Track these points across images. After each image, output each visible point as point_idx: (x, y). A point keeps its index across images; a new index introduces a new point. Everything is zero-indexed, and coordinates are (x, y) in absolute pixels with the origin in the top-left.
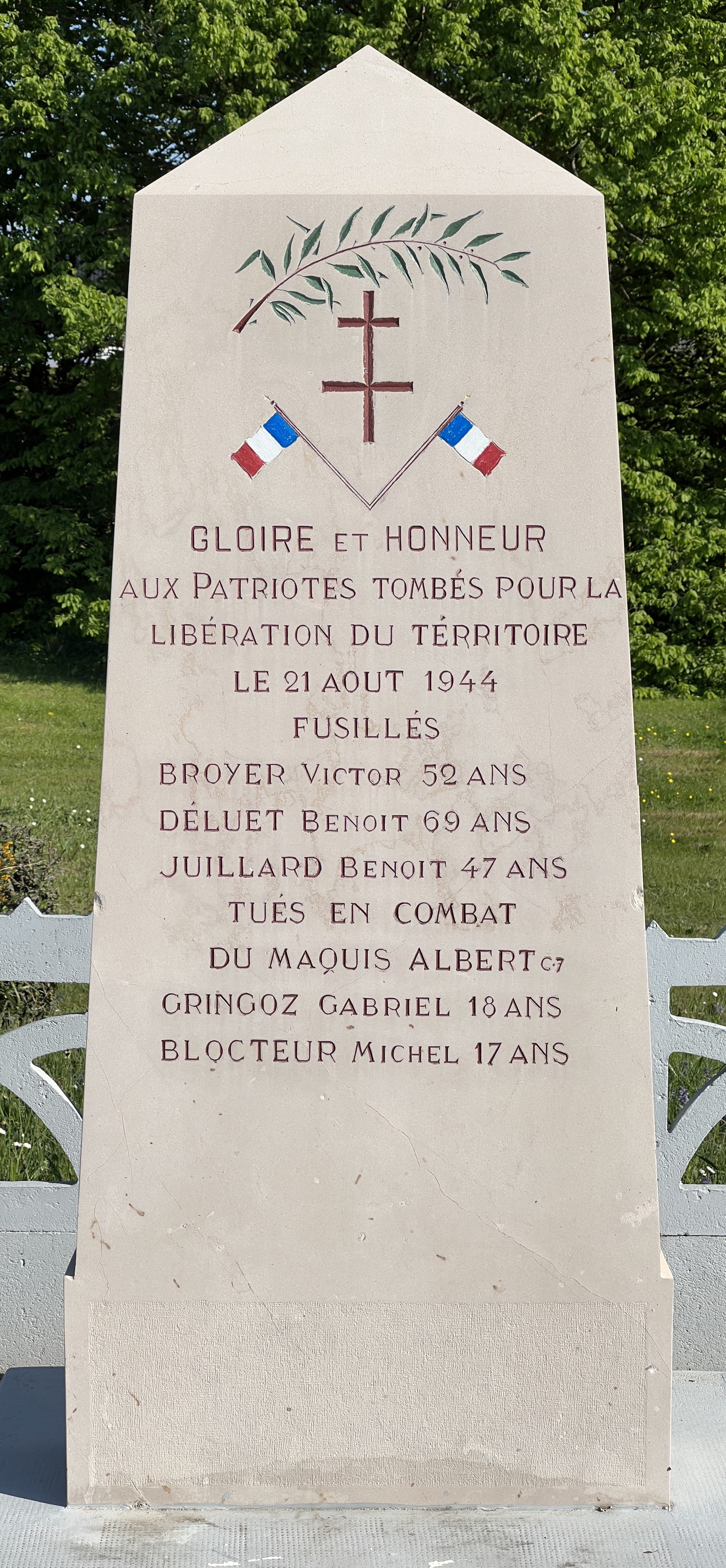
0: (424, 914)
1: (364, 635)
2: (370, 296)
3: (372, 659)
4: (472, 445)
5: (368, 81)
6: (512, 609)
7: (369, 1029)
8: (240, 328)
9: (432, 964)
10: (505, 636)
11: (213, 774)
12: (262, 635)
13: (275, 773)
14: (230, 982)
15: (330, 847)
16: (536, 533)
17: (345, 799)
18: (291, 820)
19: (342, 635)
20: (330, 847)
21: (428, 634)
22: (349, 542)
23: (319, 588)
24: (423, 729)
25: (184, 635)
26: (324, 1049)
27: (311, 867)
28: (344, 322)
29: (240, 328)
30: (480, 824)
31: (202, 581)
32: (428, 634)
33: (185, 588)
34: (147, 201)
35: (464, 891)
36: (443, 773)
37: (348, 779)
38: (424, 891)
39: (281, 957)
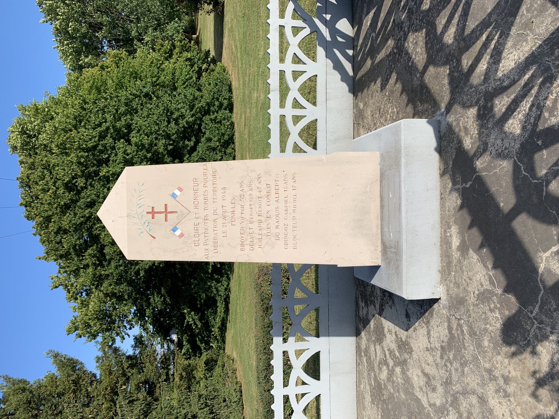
0: (268, 200)
1: (215, 213)
2: (147, 213)
3: (220, 211)
4: (177, 192)
6: (209, 184)
7: (290, 210)
8: (154, 238)
9: (278, 199)
10: (215, 186)
11: (243, 241)
12: (215, 232)
14: (282, 236)
15: (256, 218)
16: (195, 180)
17: (247, 216)
18: (251, 226)
19: (215, 217)
20: (256, 218)
21: (215, 200)
22: (197, 216)
23: (206, 221)
24: (233, 201)
25: (215, 247)
27: (260, 222)
28: (153, 218)
29: (154, 238)
30: (251, 190)
31: (205, 244)
32: (215, 200)
33: (206, 247)
34: (129, 256)
35: (264, 193)
36: (242, 197)
37: (243, 215)
38: (264, 201)
39: (277, 227)
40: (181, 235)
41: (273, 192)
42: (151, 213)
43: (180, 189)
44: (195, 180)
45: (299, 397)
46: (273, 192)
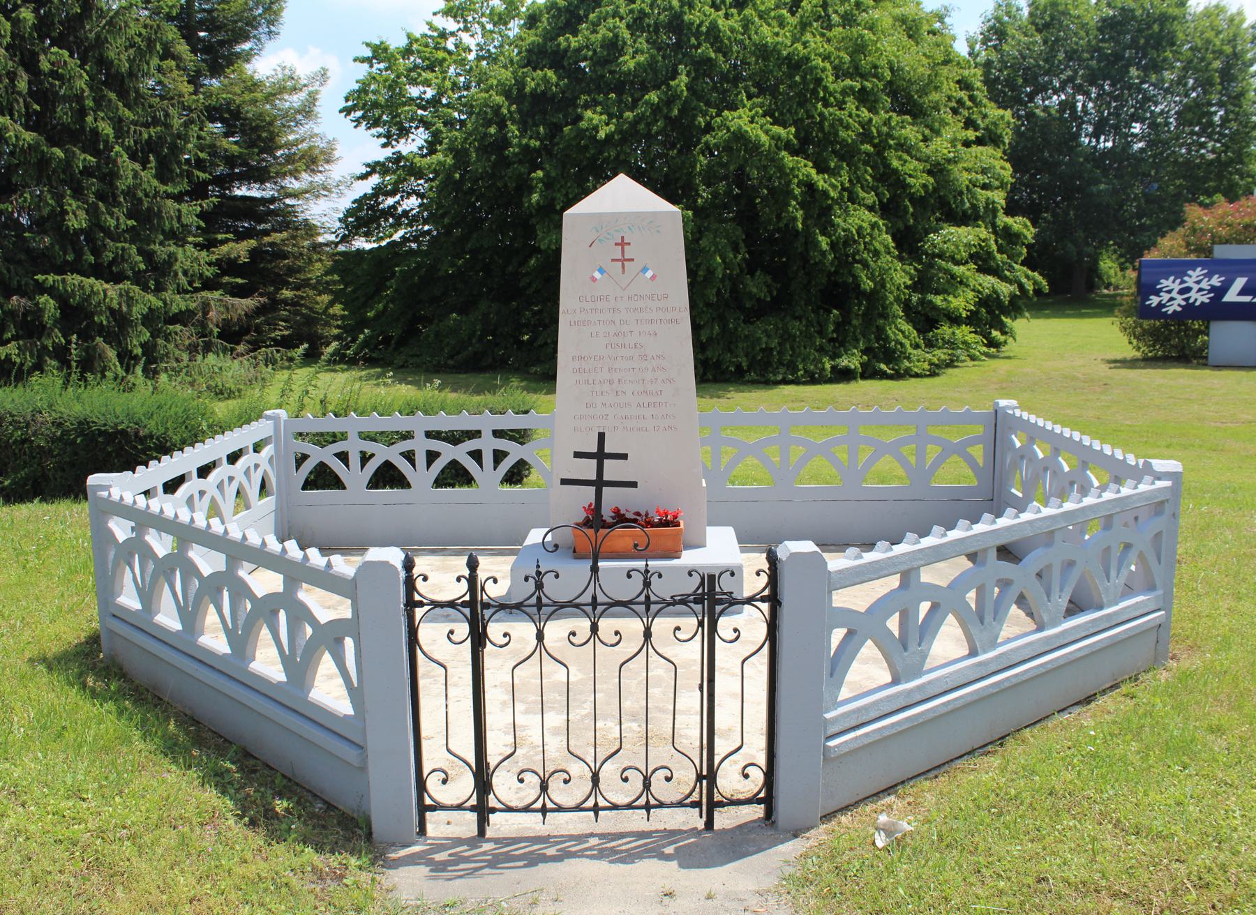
1: (623, 322)
4: (649, 274)
5: (622, 183)
13: (602, 358)
19: (617, 323)
25: (577, 323)
27: (611, 382)
28: (616, 244)
30: (654, 370)
33: (578, 311)
36: (644, 357)
39: (604, 405)
40: (594, 279)
42: (623, 248)
43: (653, 278)
44: (666, 297)
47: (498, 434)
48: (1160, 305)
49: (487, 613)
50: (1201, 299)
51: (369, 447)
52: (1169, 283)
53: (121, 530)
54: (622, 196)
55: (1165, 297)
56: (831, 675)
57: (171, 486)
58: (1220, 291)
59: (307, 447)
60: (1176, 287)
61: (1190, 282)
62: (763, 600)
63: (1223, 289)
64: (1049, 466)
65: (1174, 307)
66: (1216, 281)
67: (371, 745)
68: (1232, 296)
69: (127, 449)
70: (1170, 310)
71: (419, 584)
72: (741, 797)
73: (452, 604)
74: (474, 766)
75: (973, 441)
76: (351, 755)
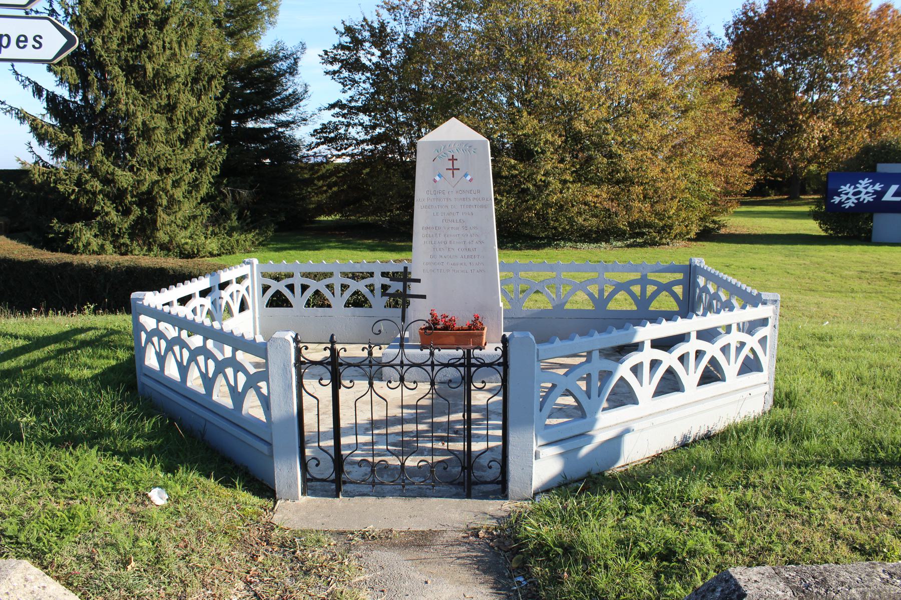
4: (469, 178)
25: (425, 207)
26: (448, 271)
27: (445, 243)
40: (435, 181)
41: (470, 253)
43: (471, 180)
45: (291, 287)
46: (470, 253)
47: (384, 274)
48: (841, 203)
49: (341, 369)
50: (869, 199)
51: (306, 281)
52: (847, 188)
53: (149, 323)
54: (454, 131)
55: (844, 197)
56: (541, 410)
57: (183, 301)
58: (880, 194)
59: (269, 282)
60: (851, 190)
61: (860, 188)
62: (499, 365)
63: (883, 193)
64: (716, 296)
65: (849, 204)
66: (878, 187)
67: (274, 444)
68: (888, 197)
69: (160, 279)
70: (847, 206)
71: (303, 351)
72: (488, 480)
73: (320, 363)
74: (333, 455)
75: (676, 283)
76: (264, 449)
